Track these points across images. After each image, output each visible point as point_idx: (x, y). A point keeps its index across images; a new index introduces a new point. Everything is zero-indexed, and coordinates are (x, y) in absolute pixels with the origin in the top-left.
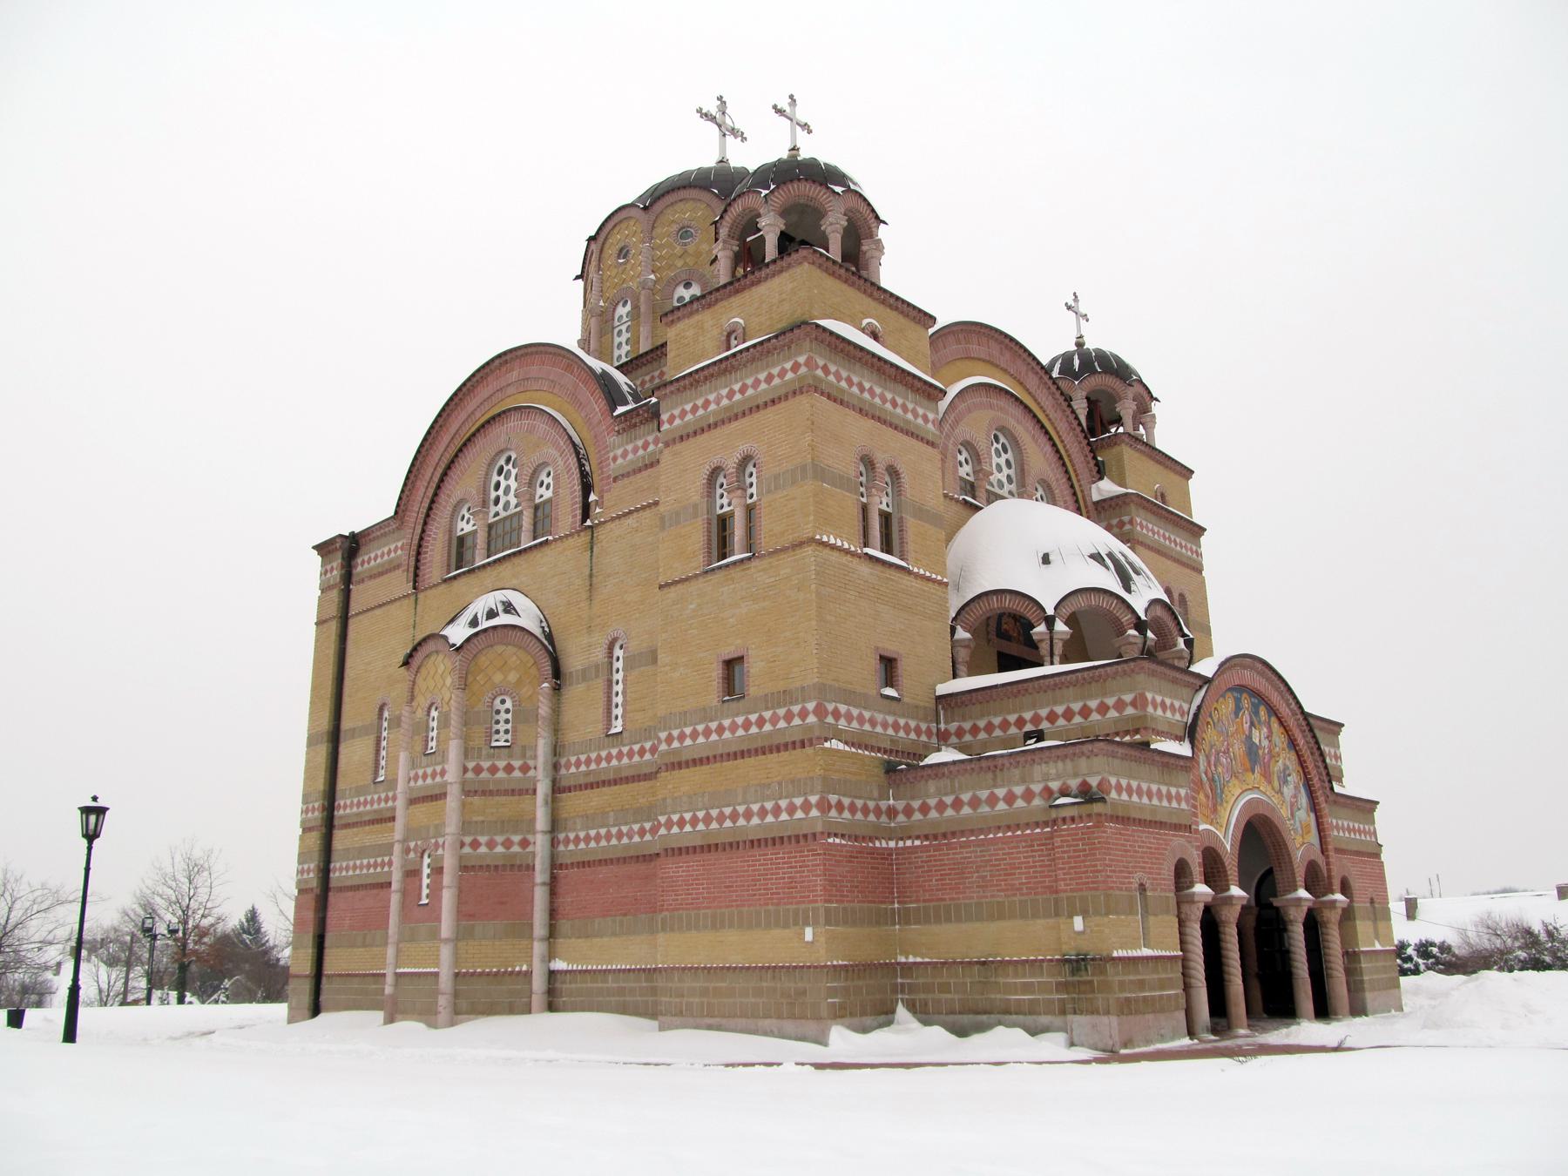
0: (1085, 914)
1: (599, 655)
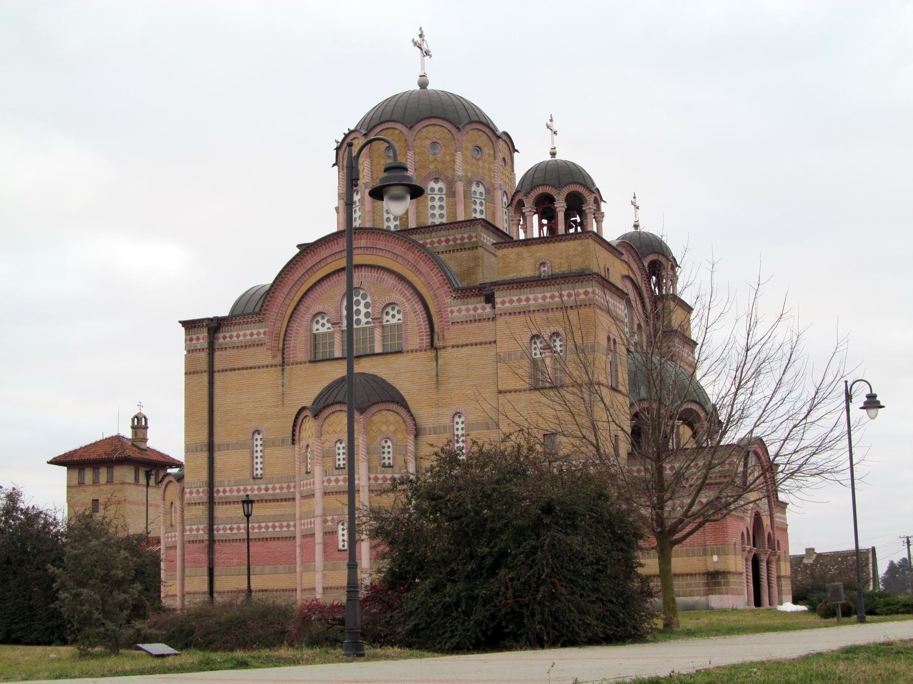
0: (719, 555)
1: (446, 421)
